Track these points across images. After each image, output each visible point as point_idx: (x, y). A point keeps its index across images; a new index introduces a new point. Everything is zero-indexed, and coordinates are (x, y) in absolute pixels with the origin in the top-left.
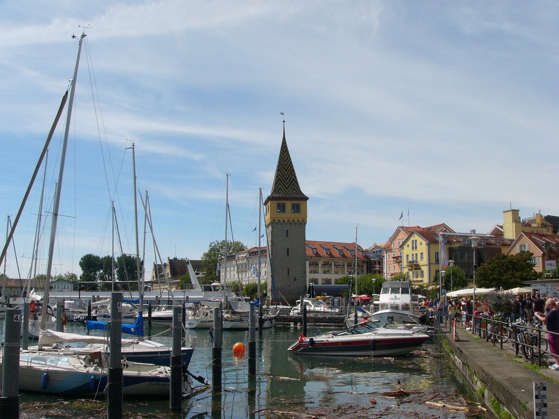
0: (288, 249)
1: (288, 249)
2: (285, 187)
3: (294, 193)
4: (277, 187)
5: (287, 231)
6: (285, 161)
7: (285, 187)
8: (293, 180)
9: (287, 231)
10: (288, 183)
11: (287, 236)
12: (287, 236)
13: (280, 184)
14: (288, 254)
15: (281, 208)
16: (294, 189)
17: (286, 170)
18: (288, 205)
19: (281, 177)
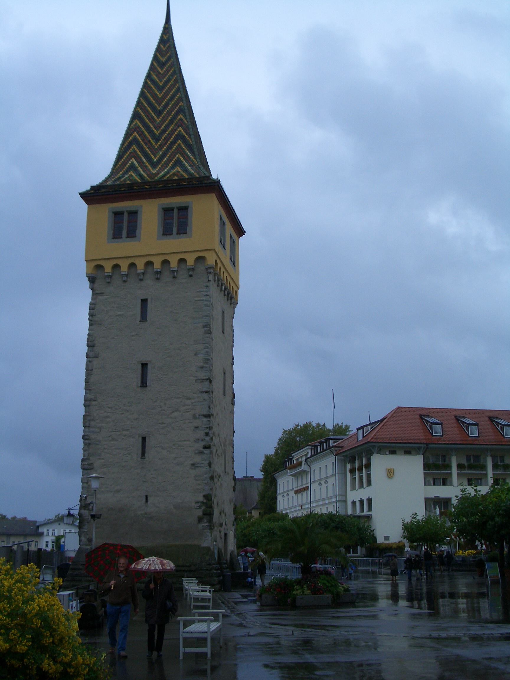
0: (144, 366)
1: (144, 366)
2: (149, 159)
3: (174, 174)
4: (124, 164)
5: (144, 302)
6: (160, 89)
7: (149, 159)
8: (180, 136)
9: (144, 302)
10: (161, 146)
11: (144, 317)
12: (144, 317)
13: (134, 155)
14: (144, 384)
15: (124, 226)
16: (178, 163)
17: (159, 113)
18: (150, 212)
19: (141, 134)
